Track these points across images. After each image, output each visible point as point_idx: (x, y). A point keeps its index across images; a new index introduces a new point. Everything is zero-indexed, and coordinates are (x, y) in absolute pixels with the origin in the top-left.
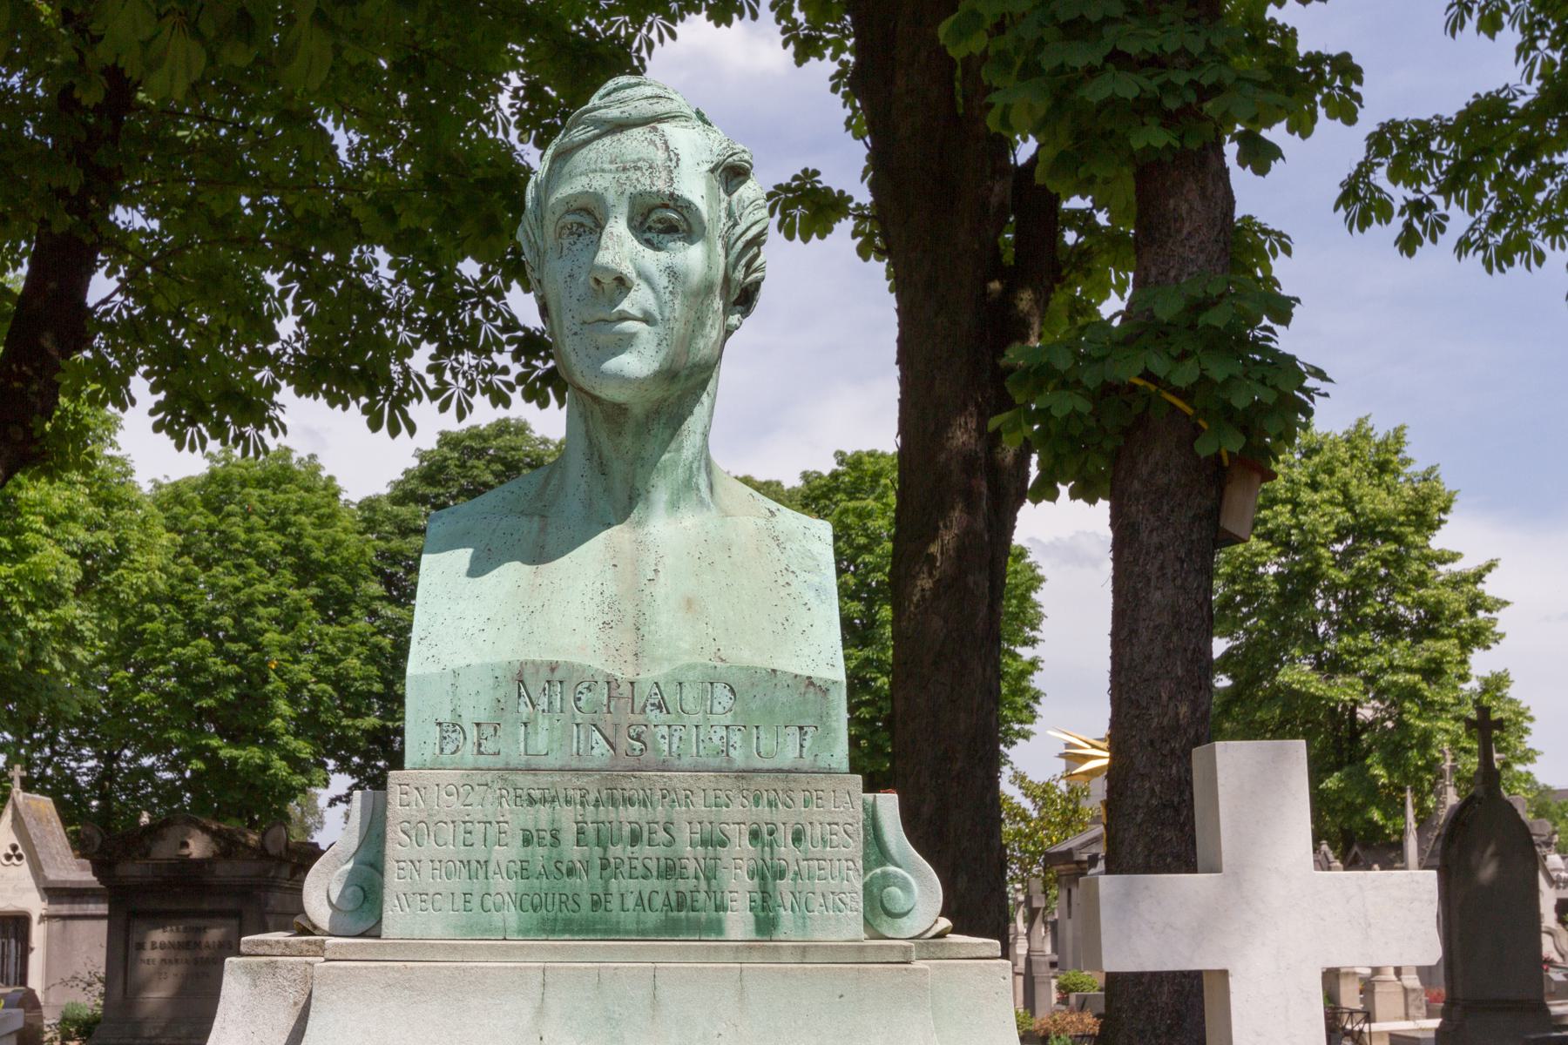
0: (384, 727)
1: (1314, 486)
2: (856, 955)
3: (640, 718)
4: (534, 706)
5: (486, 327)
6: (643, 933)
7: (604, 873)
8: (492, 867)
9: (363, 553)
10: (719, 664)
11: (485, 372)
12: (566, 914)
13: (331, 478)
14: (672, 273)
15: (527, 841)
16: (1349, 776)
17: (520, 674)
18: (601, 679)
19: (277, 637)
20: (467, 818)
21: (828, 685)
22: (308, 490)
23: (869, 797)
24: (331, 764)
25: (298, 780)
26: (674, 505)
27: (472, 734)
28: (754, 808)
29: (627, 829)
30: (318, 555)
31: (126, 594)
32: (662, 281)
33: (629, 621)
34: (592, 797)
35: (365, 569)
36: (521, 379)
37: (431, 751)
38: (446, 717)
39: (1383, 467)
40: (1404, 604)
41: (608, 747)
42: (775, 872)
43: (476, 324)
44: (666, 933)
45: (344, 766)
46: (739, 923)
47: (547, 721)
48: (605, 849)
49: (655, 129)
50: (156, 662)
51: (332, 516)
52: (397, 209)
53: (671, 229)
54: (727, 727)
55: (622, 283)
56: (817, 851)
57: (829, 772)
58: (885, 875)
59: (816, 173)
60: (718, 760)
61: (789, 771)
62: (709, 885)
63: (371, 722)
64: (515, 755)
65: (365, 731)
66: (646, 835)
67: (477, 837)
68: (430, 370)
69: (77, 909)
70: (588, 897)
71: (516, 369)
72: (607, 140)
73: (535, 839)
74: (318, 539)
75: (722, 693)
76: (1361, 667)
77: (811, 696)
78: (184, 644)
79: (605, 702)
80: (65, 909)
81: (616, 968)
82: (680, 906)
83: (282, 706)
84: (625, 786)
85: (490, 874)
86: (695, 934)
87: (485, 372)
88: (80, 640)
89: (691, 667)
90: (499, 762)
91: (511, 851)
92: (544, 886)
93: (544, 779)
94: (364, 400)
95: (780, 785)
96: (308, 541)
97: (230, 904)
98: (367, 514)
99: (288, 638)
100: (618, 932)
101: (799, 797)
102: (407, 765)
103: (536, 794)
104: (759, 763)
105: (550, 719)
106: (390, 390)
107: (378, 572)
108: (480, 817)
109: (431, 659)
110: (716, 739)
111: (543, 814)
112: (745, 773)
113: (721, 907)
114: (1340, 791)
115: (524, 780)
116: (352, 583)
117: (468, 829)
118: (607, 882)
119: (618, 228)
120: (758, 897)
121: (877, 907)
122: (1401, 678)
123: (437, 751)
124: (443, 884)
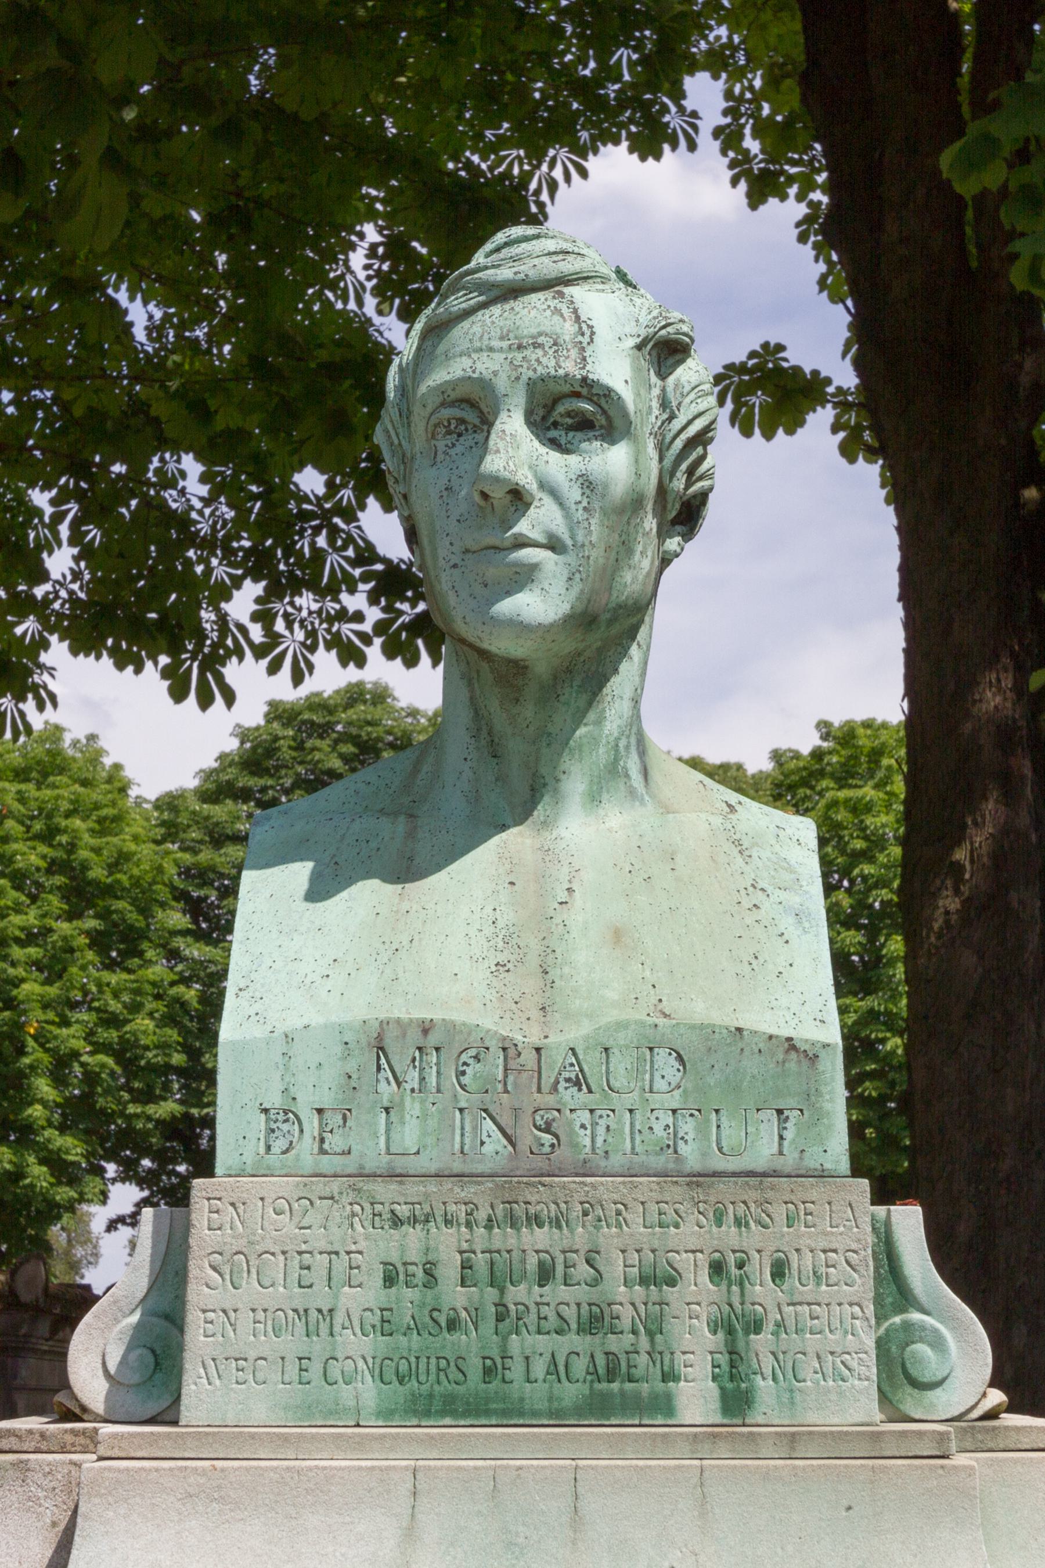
0: (187, 1116)
3: (550, 1100)
4: (399, 1084)
7: (501, 1326)
8: (339, 1318)
9: (160, 870)
10: (661, 1021)
12: (446, 1387)
13: (117, 767)
15: (389, 1280)
17: (380, 1037)
18: (493, 1044)
19: (37, 988)
20: (304, 1247)
21: (817, 1049)
22: (85, 783)
23: (881, 1210)
24: (111, 1169)
25: (64, 1193)
26: (594, 798)
27: (312, 1124)
28: (714, 1229)
29: (532, 1261)
30: (97, 873)
33: (533, 961)
34: (482, 1215)
35: (162, 893)
37: (252, 1150)
38: (274, 1100)
41: (505, 1142)
42: (748, 1323)
44: (592, 1414)
45: (129, 1173)
47: (417, 1105)
48: (502, 1291)
51: (117, 819)
54: (674, 1111)
56: (807, 1291)
57: (822, 1175)
58: (907, 1326)
60: (662, 1159)
61: (764, 1175)
62: (652, 1341)
63: (168, 1108)
65: (159, 1122)
66: (560, 1269)
67: (318, 1276)
70: (477, 1362)
73: (402, 1277)
74: (97, 851)
75: (666, 1064)
77: (792, 1066)
79: (500, 1077)
81: (520, 1468)
82: (612, 1374)
83: (44, 1087)
84: (533, 1199)
85: (337, 1329)
86: (633, 1416)
90: (350, 1164)
92: (415, 1346)
93: (414, 1189)
95: (752, 1195)
96: (84, 854)
98: (166, 815)
99: (53, 991)
100: (521, 1414)
101: (779, 1212)
102: (219, 1170)
103: (403, 1211)
104: (721, 1164)
105: (423, 1102)
107: (180, 895)
108: (322, 1245)
109: (254, 1018)
110: (658, 1128)
111: (413, 1237)
113: (669, 1376)
115: (385, 1191)
116: (145, 912)
117: (306, 1263)
118: (505, 1339)
120: (723, 1359)
123: (262, 1150)
124: (268, 1344)
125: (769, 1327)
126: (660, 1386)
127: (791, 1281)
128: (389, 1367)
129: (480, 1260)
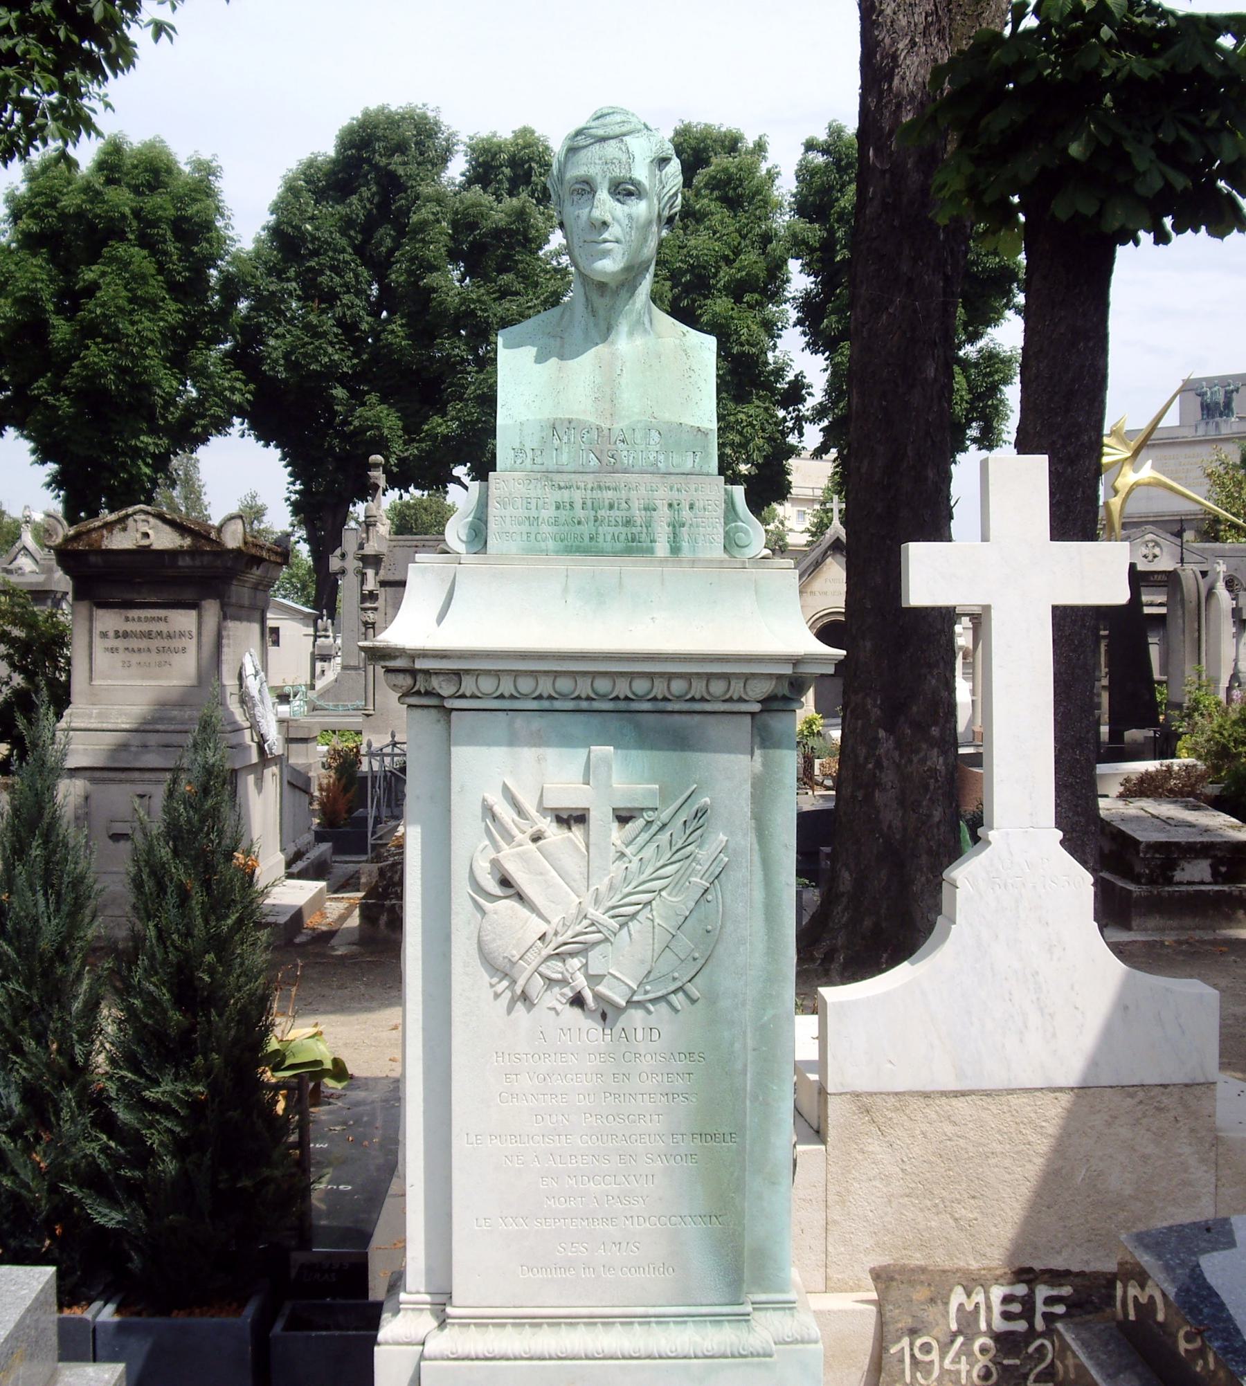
2: (720, 564)
6: (615, 554)
8: (540, 520)
14: (630, 217)
15: (558, 508)
18: (593, 427)
23: (729, 487)
26: (631, 333)
27: (530, 453)
34: (589, 486)
37: (510, 462)
38: (517, 446)
46: (662, 548)
49: (622, 141)
53: (630, 194)
57: (708, 475)
58: (736, 527)
64: (551, 464)
72: (597, 146)
75: (654, 434)
77: (699, 436)
89: (639, 421)
91: (549, 513)
93: (566, 477)
102: (498, 469)
103: (562, 484)
110: (651, 458)
111: (566, 493)
115: (558, 478)
119: (603, 195)
120: (672, 536)
121: (731, 543)
124: (516, 528)
125: (687, 526)
126: (650, 544)
127: (696, 510)
128: (558, 539)
129: (589, 502)
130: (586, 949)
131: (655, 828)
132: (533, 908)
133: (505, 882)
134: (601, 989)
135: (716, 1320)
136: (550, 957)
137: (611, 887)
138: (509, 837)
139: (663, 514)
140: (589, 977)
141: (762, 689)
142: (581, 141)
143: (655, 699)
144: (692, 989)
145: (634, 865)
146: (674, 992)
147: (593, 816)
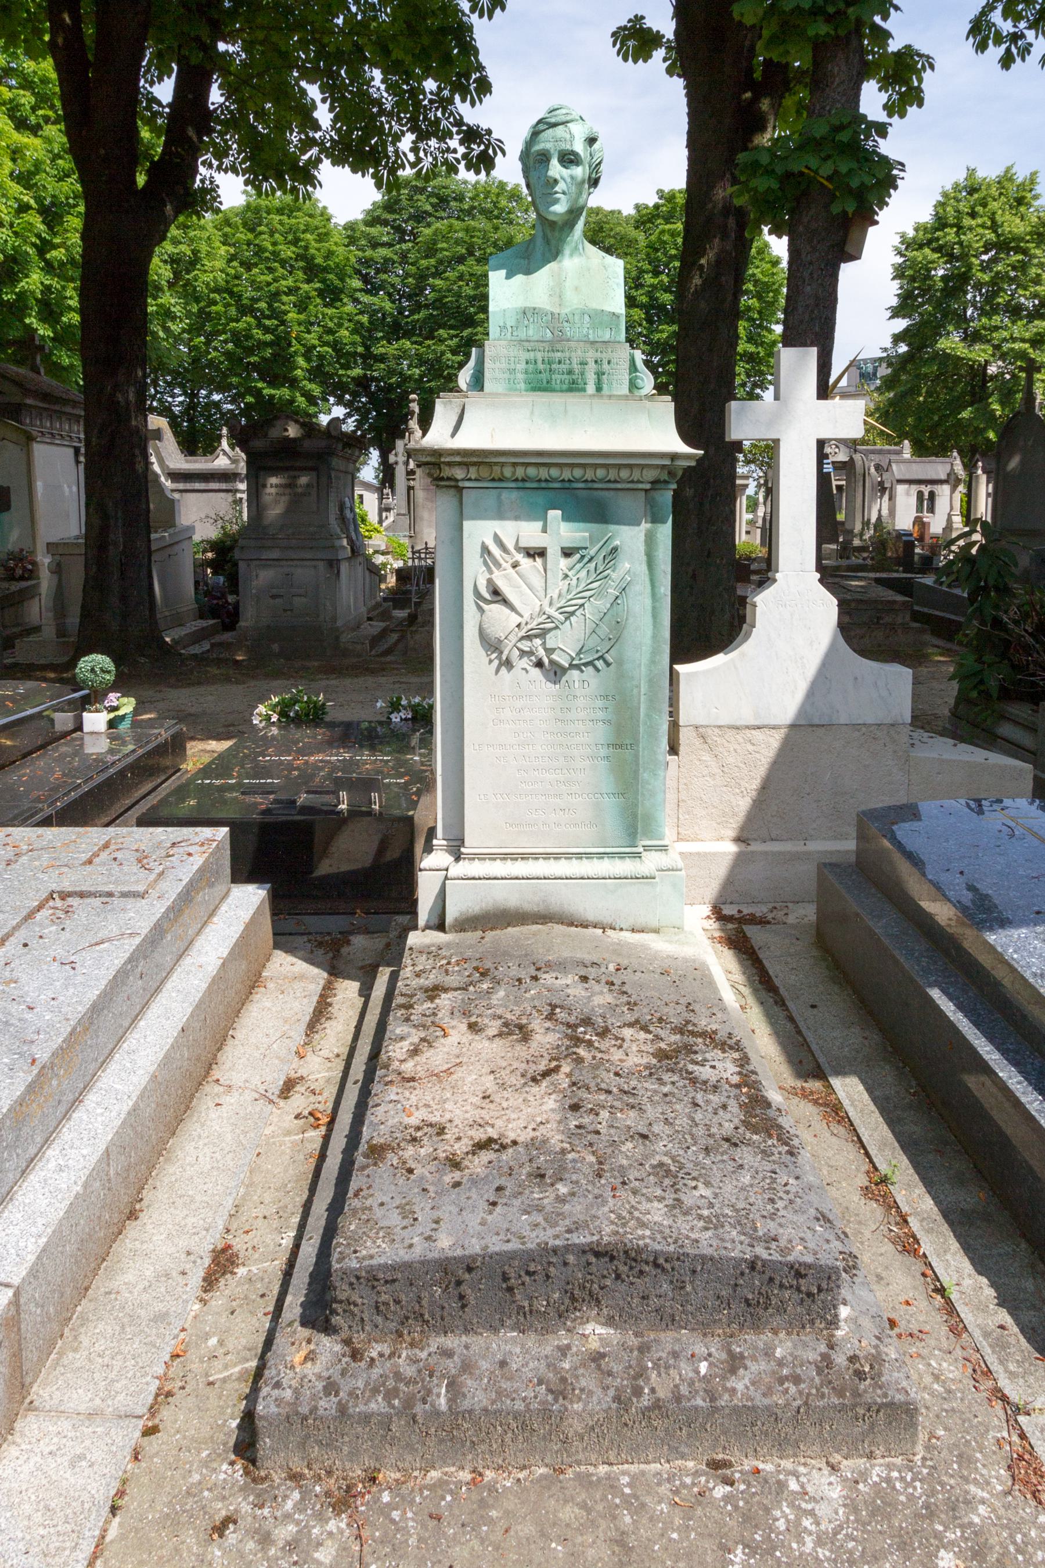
0: (365, 375)
1: (973, 215)
2: (626, 398)
5: (444, 123)
9: (348, 259)
11: (443, 152)
13: (325, 208)
14: (572, 177)
16: (977, 410)
19: (296, 316)
22: (311, 216)
24: (332, 400)
25: (312, 410)
26: (571, 255)
30: (319, 260)
31: (200, 287)
32: (569, 180)
35: (349, 270)
36: (465, 156)
39: (1020, 201)
40: (1024, 296)
43: (438, 121)
45: (340, 402)
46: (591, 388)
50: (219, 333)
51: (327, 234)
52: (391, 47)
53: (571, 162)
55: (556, 181)
59: (642, 17)
63: (357, 372)
64: (523, 336)
65: (353, 379)
68: (412, 150)
69: (189, 486)
71: (462, 150)
74: (318, 250)
75: (587, 317)
76: (992, 339)
78: (237, 321)
80: (181, 486)
83: (301, 361)
87: (443, 152)
88: (173, 318)
91: (522, 366)
94: (371, 171)
96: (312, 251)
97: (310, 464)
98: (349, 233)
99: (302, 317)
106: (387, 163)
107: (358, 272)
111: (532, 354)
112: (593, 343)
114: (970, 419)
115: (526, 344)
116: (342, 280)
119: (554, 162)
121: (633, 386)
122: (1017, 346)
124: (501, 376)
130: (543, 634)
131: (586, 560)
132: (513, 608)
133: (496, 592)
134: (554, 657)
135: (621, 856)
136: (522, 638)
137: (560, 595)
138: (498, 565)
139: (591, 368)
140: (546, 650)
141: (650, 475)
142: (541, 127)
143: (586, 481)
144: (608, 657)
145: (574, 582)
146: (598, 659)
147: (550, 552)
